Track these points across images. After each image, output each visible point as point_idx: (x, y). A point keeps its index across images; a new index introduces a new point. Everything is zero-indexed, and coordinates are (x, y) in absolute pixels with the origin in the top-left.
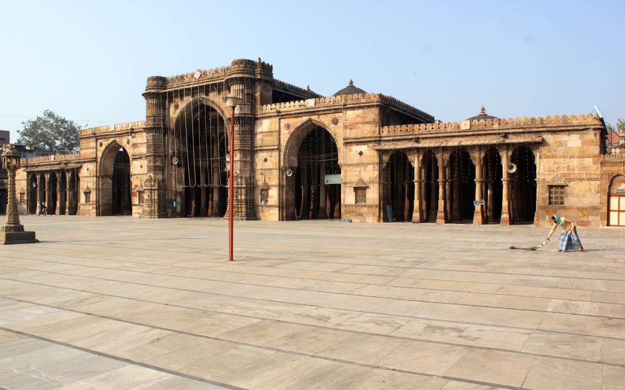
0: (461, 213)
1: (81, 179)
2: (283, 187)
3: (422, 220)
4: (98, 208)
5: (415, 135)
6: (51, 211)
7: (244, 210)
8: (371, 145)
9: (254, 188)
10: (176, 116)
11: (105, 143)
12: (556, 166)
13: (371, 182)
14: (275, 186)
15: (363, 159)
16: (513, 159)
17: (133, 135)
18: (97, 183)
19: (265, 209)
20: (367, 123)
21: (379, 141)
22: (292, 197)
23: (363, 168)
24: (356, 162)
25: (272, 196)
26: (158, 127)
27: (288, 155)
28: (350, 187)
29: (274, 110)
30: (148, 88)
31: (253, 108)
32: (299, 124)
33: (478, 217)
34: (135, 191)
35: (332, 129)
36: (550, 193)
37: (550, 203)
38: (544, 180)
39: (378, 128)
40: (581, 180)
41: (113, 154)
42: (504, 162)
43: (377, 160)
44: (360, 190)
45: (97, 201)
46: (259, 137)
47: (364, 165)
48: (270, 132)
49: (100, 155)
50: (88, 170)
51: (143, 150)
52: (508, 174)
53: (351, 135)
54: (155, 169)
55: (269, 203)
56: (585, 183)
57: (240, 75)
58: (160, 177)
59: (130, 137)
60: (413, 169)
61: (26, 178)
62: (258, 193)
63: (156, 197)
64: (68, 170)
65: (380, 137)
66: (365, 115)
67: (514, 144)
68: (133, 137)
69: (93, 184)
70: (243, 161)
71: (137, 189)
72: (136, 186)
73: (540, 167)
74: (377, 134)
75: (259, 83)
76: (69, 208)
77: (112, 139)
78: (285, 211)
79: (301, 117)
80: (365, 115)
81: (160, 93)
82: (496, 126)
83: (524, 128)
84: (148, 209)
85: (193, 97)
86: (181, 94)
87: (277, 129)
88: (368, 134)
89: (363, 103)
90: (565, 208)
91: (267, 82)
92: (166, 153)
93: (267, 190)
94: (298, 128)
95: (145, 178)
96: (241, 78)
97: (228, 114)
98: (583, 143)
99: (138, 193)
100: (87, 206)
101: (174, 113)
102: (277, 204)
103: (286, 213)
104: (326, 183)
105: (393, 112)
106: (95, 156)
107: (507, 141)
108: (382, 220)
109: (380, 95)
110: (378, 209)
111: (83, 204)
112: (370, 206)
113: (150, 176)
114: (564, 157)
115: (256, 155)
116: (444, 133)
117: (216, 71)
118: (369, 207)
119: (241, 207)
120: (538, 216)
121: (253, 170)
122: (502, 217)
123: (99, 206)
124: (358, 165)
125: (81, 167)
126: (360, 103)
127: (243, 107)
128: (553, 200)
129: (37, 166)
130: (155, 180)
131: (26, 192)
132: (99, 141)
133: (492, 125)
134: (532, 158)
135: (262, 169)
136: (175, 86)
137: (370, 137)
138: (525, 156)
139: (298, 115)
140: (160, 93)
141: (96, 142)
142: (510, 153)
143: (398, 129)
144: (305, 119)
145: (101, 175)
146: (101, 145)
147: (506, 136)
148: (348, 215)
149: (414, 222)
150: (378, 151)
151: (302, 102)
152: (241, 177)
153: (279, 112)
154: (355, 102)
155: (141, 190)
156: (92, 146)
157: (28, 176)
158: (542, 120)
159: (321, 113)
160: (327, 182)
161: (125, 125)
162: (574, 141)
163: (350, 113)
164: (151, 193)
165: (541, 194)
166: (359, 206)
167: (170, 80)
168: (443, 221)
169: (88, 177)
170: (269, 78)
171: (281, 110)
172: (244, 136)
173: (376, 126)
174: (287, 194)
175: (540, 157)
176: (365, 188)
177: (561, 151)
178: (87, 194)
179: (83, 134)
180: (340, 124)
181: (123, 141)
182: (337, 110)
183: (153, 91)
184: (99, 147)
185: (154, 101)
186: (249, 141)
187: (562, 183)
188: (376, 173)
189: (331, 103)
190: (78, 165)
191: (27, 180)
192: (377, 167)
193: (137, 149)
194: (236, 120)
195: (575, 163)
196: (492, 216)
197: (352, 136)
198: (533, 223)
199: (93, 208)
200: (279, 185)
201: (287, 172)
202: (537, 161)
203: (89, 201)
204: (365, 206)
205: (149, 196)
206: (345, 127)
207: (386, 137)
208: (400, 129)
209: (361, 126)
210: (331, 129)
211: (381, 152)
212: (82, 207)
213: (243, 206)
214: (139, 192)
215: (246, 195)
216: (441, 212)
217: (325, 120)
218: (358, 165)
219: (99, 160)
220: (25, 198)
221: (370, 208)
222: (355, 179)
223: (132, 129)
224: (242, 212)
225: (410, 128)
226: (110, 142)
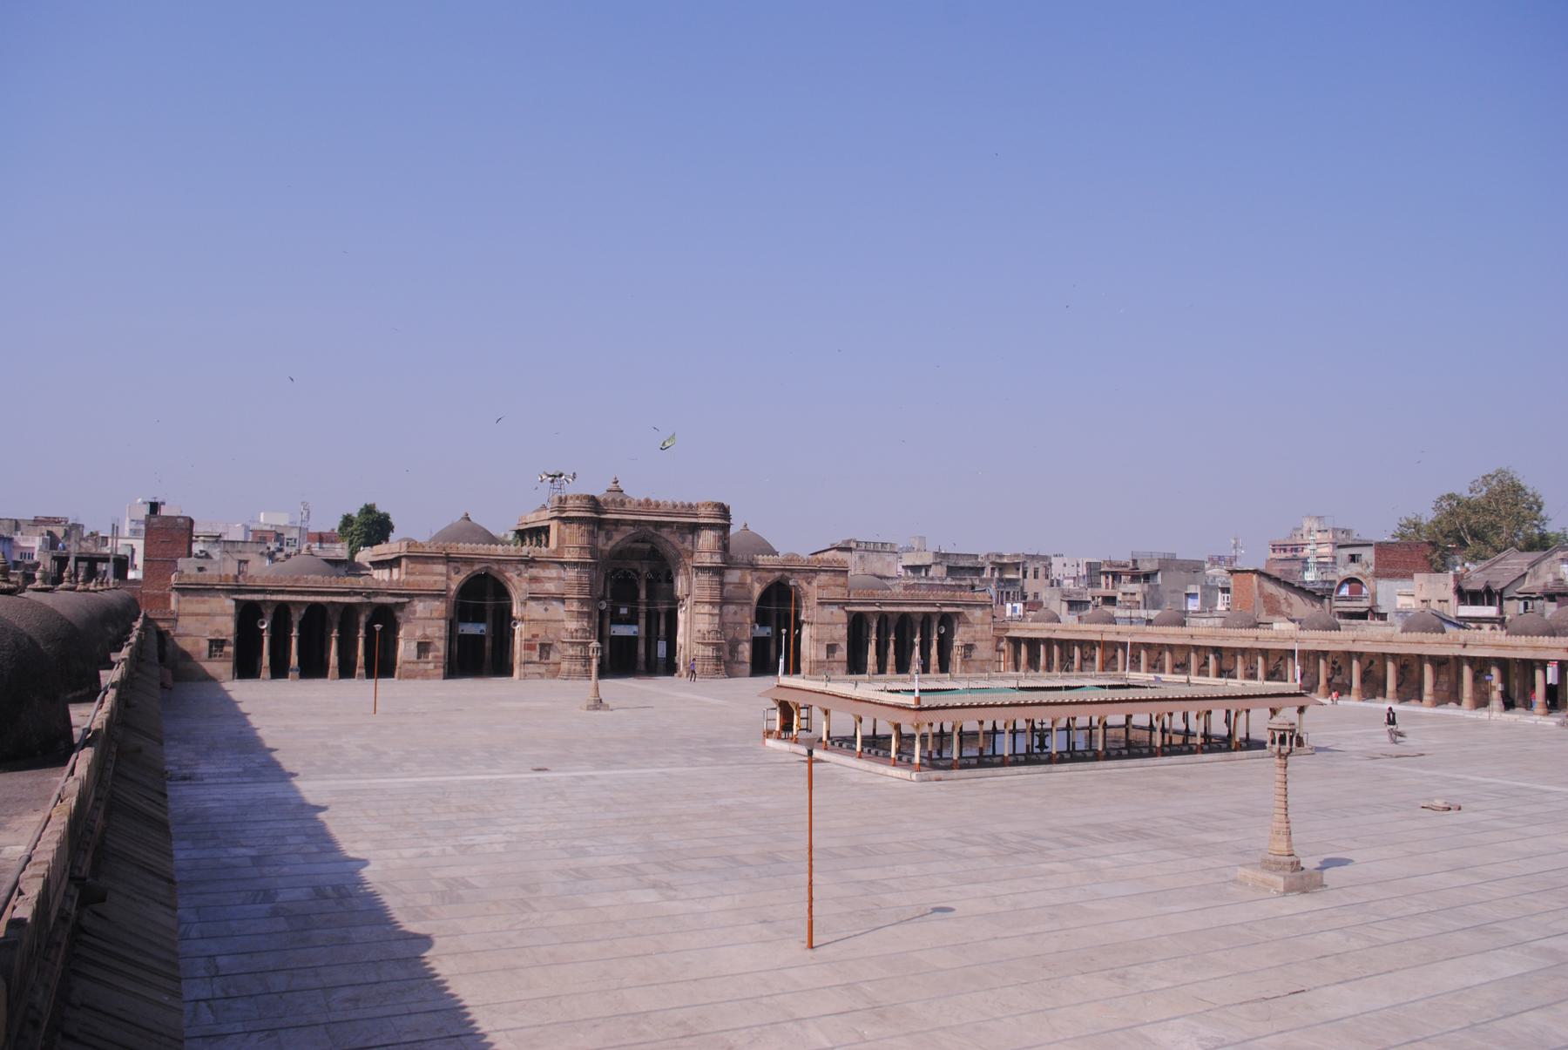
15: (835, 620)
46: (727, 588)
49: (454, 587)
52: (939, 635)
54: (589, 615)
59: (522, 567)
61: (232, 611)
84: (579, 668)
100: (422, 666)
131: (231, 639)
144: (778, 574)
162: (978, 613)
180: (815, 583)
195: (978, 628)
214: (543, 646)
220: (230, 649)
226: (476, 567)
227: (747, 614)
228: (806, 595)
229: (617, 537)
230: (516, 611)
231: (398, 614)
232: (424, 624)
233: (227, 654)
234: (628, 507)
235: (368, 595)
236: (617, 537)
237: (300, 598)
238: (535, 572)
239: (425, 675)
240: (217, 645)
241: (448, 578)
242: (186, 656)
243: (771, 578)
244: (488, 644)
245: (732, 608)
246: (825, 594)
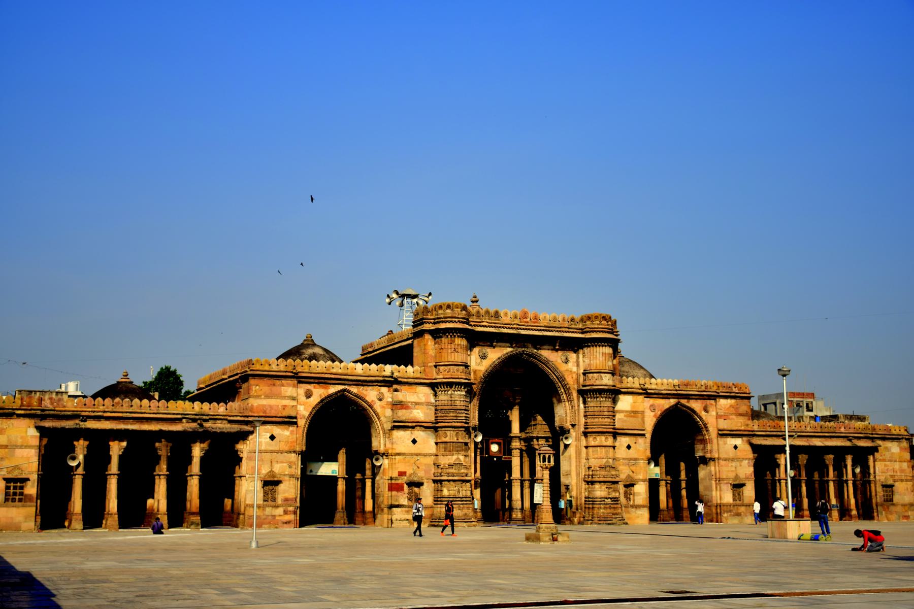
1: (244, 455)
8: (745, 439)
11: (319, 393)
13: (747, 478)
14: (644, 481)
15: (738, 453)
17: (395, 386)
19: (630, 509)
20: (741, 415)
23: (738, 464)
25: (639, 494)
32: (667, 406)
34: (399, 482)
35: (704, 418)
40: (902, 480)
43: (751, 455)
47: (740, 460)
48: (633, 412)
50: (272, 437)
55: (631, 503)
56: (904, 483)
59: (384, 390)
68: (396, 390)
69: (290, 467)
71: (404, 479)
72: (402, 474)
77: (343, 387)
90: (893, 505)
93: (633, 485)
97: (570, 380)
98: (901, 449)
99: (406, 486)
100: (268, 511)
106: (293, 414)
113: (458, 459)
114: (891, 461)
124: (733, 460)
131: (34, 477)
135: (624, 459)
136: (484, 324)
144: (673, 401)
146: (309, 395)
148: (725, 515)
153: (645, 390)
155: (416, 479)
156: (288, 394)
162: (895, 448)
163: (722, 402)
165: (878, 494)
169: (272, 452)
175: (875, 461)
176: (742, 485)
179: (258, 367)
182: (710, 397)
185: (464, 342)
187: (890, 482)
188: (752, 469)
189: (703, 388)
192: (752, 463)
193: (404, 411)
195: (897, 466)
197: (725, 427)
199: (286, 512)
203: (274, 500)
205: (459, 491)
206: (718, 417)
209: (734, 417)
211: (755, 448)
214: (412, 484)
217: (696, 405)
219: (302, 422)
220: (31, 489)
222: (732, 475)
226: (333, 389)
227: (643, 447)
228: (705, 425)
230: (379, 443)
231: (240, 446)
232: (269, 458)
233: (29, 498)
237: (122, 426)
238: (400, 396)
239: (272, 522)
240: (15, 484)
244: (341, 486)
245: (623, 441)
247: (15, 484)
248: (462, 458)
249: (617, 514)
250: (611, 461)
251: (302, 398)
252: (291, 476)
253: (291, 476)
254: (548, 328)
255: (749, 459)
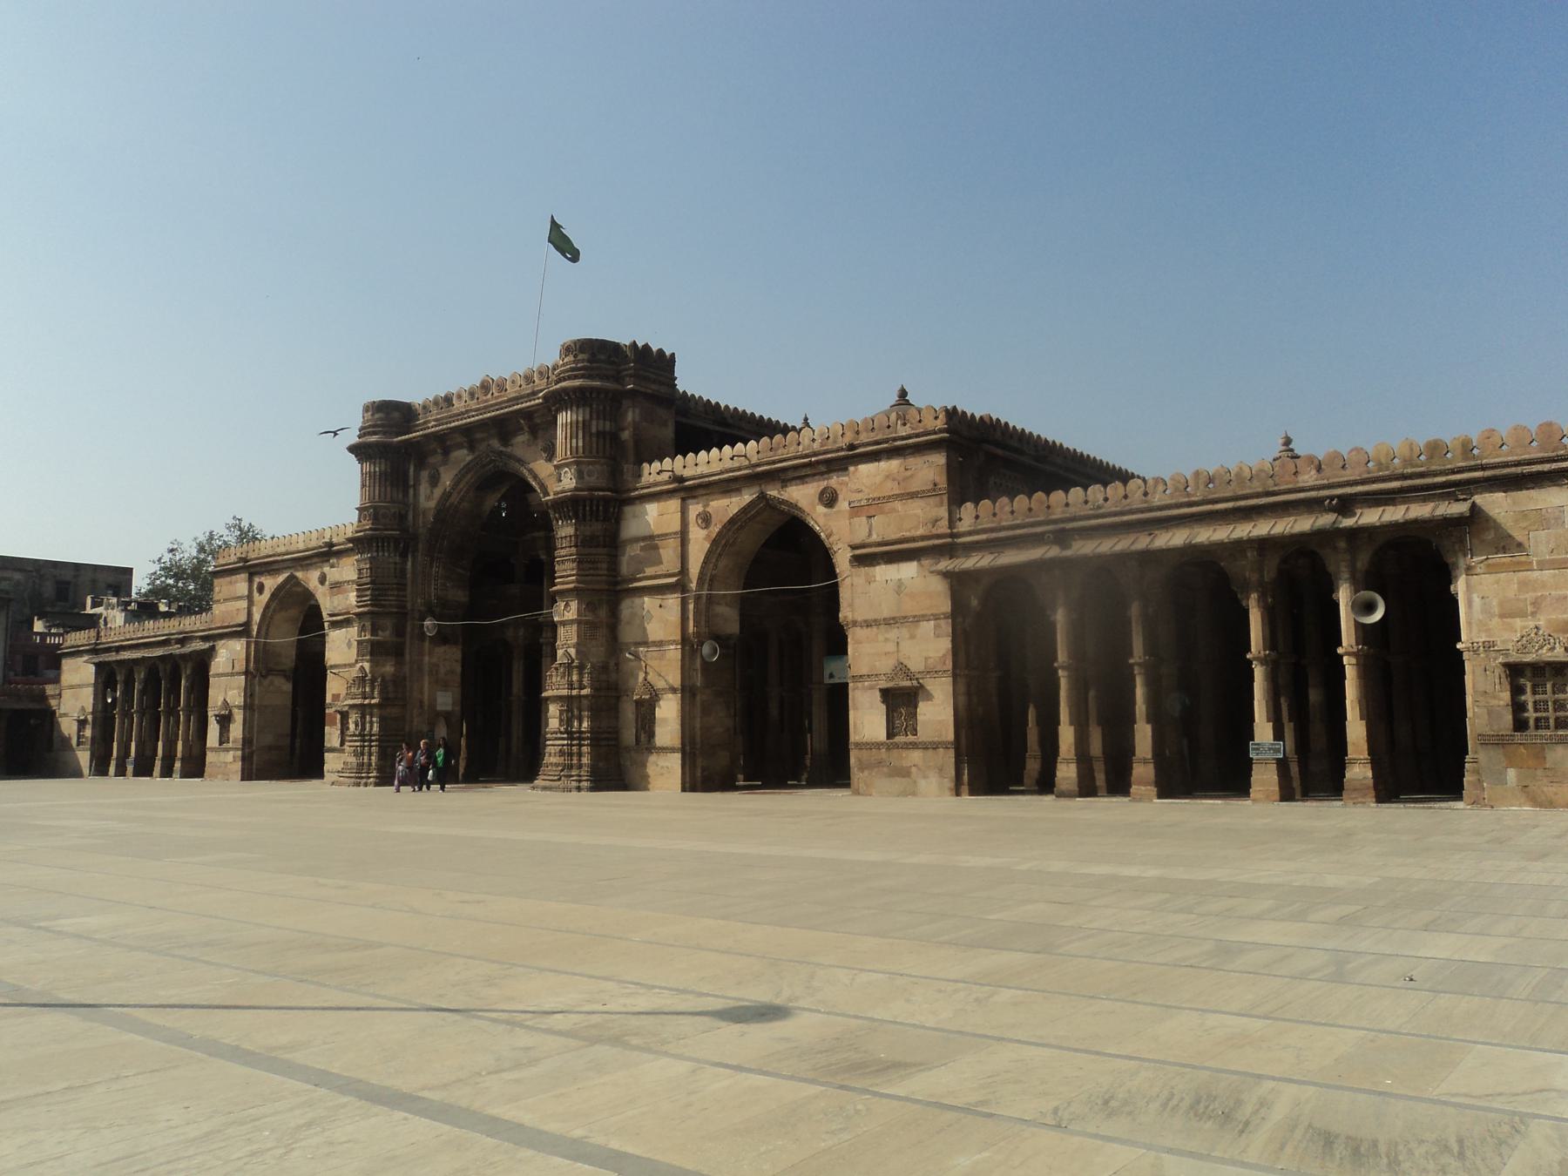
0: (1207, 764)
2: (694, 695)
3: (1087, 788)
4: (246, 759)
5: (1055, 522)
6: (144, 770)
7: (585, 760)
8: (926, 562)
9: (618, 698)
10: (432, 504)
11: (271, 583)
12: (1530, 596)
13: (932, 672)
14: (674, 690)
16: (1371, 580)
18: (249, 693)
20: (913, 495)
21: (948, 548)
22: (721, 721)
23: (904, 632)
24: (886, 613)
25: (665, 720)
26: (386, 535)
27: (706, 606)
28: (871, 688)
29: (665, 476)
30: (364, 432)
31: (615, 473)
33: (1264, 777)
35: (821, 521)
36: (1517, 690)
37: (1520, 725)
38: (1489, 646)
39: (945, 507)
41: (293, 612)
42: (1344, 596)
43: (946, 606)
44: (901, 701)
45: (247, 741)
49: (257, 617)
51: (350, 600)
52: (1363, 632)
53: (870, 535)
57: (577, 383)
58: (389, 669)
59: (326, 569)
60: (1053, 626)
62: (629, 713)
63: (376, 728)
64: (183, 656)
65: (952, 535)
66: (909, 473)
67: (1370, 531)
70: (587, 622)
72: (336, 697)
73: (1470, 603)
74: (943, 527)
75: (629, 398)
76: (182, 759)
77: (286, 575)
78: (700, 762)
79: (738, 491)
80: (909, 473)
81: (394, 444)
82: (1309, 478)
83: (1404, 477)
84: (353, 760)
85: (472, 448)
86: (443, 442)
87: (678, 528)
88: (917, 528)
89: (903, 438)
91: (655, 399)
92: (409, 605)
94: (732, 521)
95: (354, 672)
96: (580, 389)
101: (429, 498)
102: (677, 743)
103: (703, 770)
104: (827, 681)
105: (985, 457)
106: (242, 618)
107: (1348, 522)
108: (965, 788)
109: (952, 414)
110: (952, 753)
111: (213, 749)
112: (925, 746)
115: (627, 607)
116: (1142, 511)
117: (528, 379)
118: (925, 746)
119: (580, 755)
120: (1477, 772)
121: (614, 645)
122: (1348, 775)
123: (252, 753)
124: (890, 622)
125: (213, 648)
126: (895, 439)
127: (585, 469)
128: (1531, 714)
129: (119, 649)
130: (373, 681)
131: (90, 718)
132: (257, 580)
133: (1296, 473)
134: (1445, 576)
137: (923, 538)
138: (1417, 573)
139: (727, 485)
140: (394, 444)
141: (250, 581)
142: (1363, 561)
143: (1002, 508)
144: (747, 497)
145: (257, 669)
146: (261, 588)
147: (1345, 505)
149: (1061, 795)
150: (946, 575)
151: (739, 445)
152: (581, 668)
153: (681, 479)
154: (880, 437)
157: (97, 673)
158: (1467, 448)
159: (791, 474)
160: (831, 676)
161: (315, 535)
163: (865, 469)
164: (363, 717)
165: (1484, 698)
166: (897, 746)
167: (420, 410)
168: (1153, 790)
170: (664, 389)
171: (687, 473)
172: (587, 551)
173: (942, 504)
174: (706, 711)
177: (1540, 543)
178: (225, 721)
180: (842, 505)
181: (310, 578)
183: (374, 438)
184: (256, 594)
186: (605, 566)
188: (945, 644)
189: (816, 446)
190: (207, 645)
191: (96, 685)
192: (946, 626)
194: (571, 506)
196: (1314, 774)
197: (875, 538)
198: (1459, 797)
200: (683, 689)
201: (706, 649)
202: (1460, 587)
204: (915, 746)
206: (855, 510)
207: (970, 533)
208: (1008, 509)
209: (898, 505)
210: (819, 518)
211: (958, 582)
212: (210, 757)
213: (585, 749)
215: (592, 719)
216: (1145, 761)
217: (802, 495)
218: (890, 622)
220: (88, 732)
221: (930, 752)
222: (886, 665)
223: (331, 545)
224: (580, 767)
225: (1041, 503)
229: (447, 480)
234: (458, 406)
235: (182, 642)
236: (447, 480)
241: (250, 598)
242: (66, 741)
243: (727, 506)
246: (883, 528)
247: (82, 724)
248: (367, 666)
249: (571, 767)
250: (572, 651)
251: (256, 594)
252: (238, 707)
253: (238, 707)
254: (516, 400)
255: (936, 617)
